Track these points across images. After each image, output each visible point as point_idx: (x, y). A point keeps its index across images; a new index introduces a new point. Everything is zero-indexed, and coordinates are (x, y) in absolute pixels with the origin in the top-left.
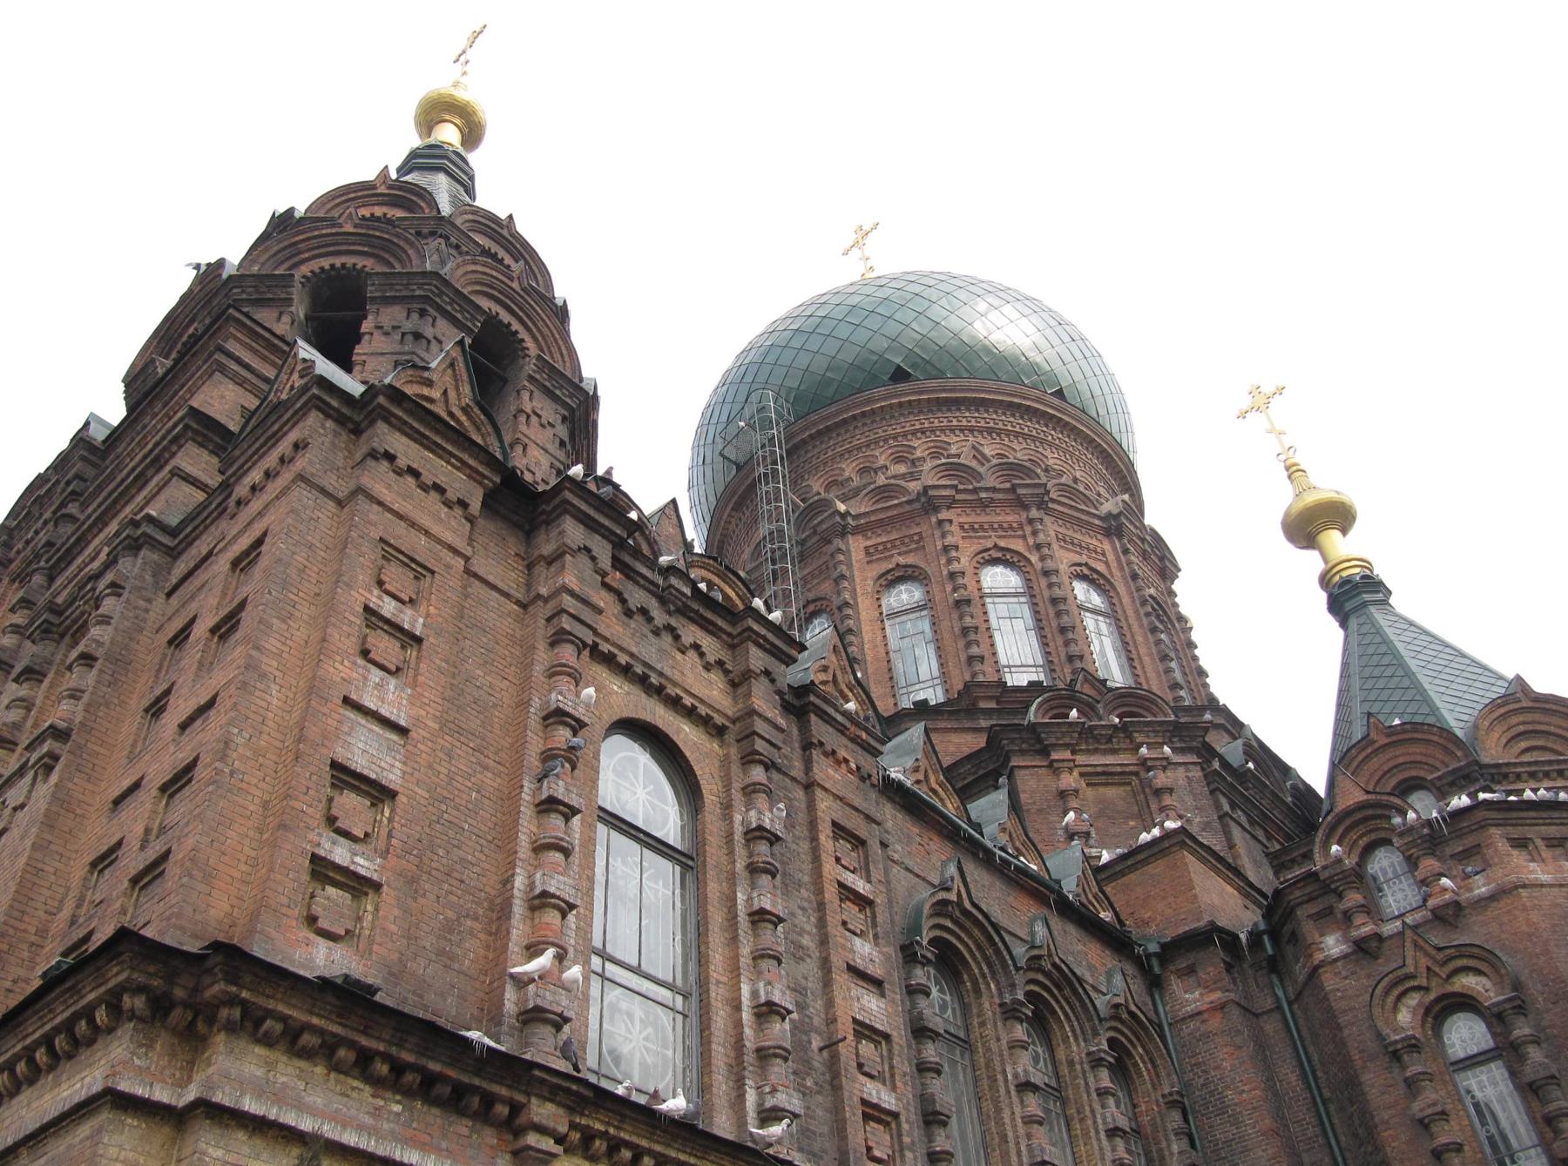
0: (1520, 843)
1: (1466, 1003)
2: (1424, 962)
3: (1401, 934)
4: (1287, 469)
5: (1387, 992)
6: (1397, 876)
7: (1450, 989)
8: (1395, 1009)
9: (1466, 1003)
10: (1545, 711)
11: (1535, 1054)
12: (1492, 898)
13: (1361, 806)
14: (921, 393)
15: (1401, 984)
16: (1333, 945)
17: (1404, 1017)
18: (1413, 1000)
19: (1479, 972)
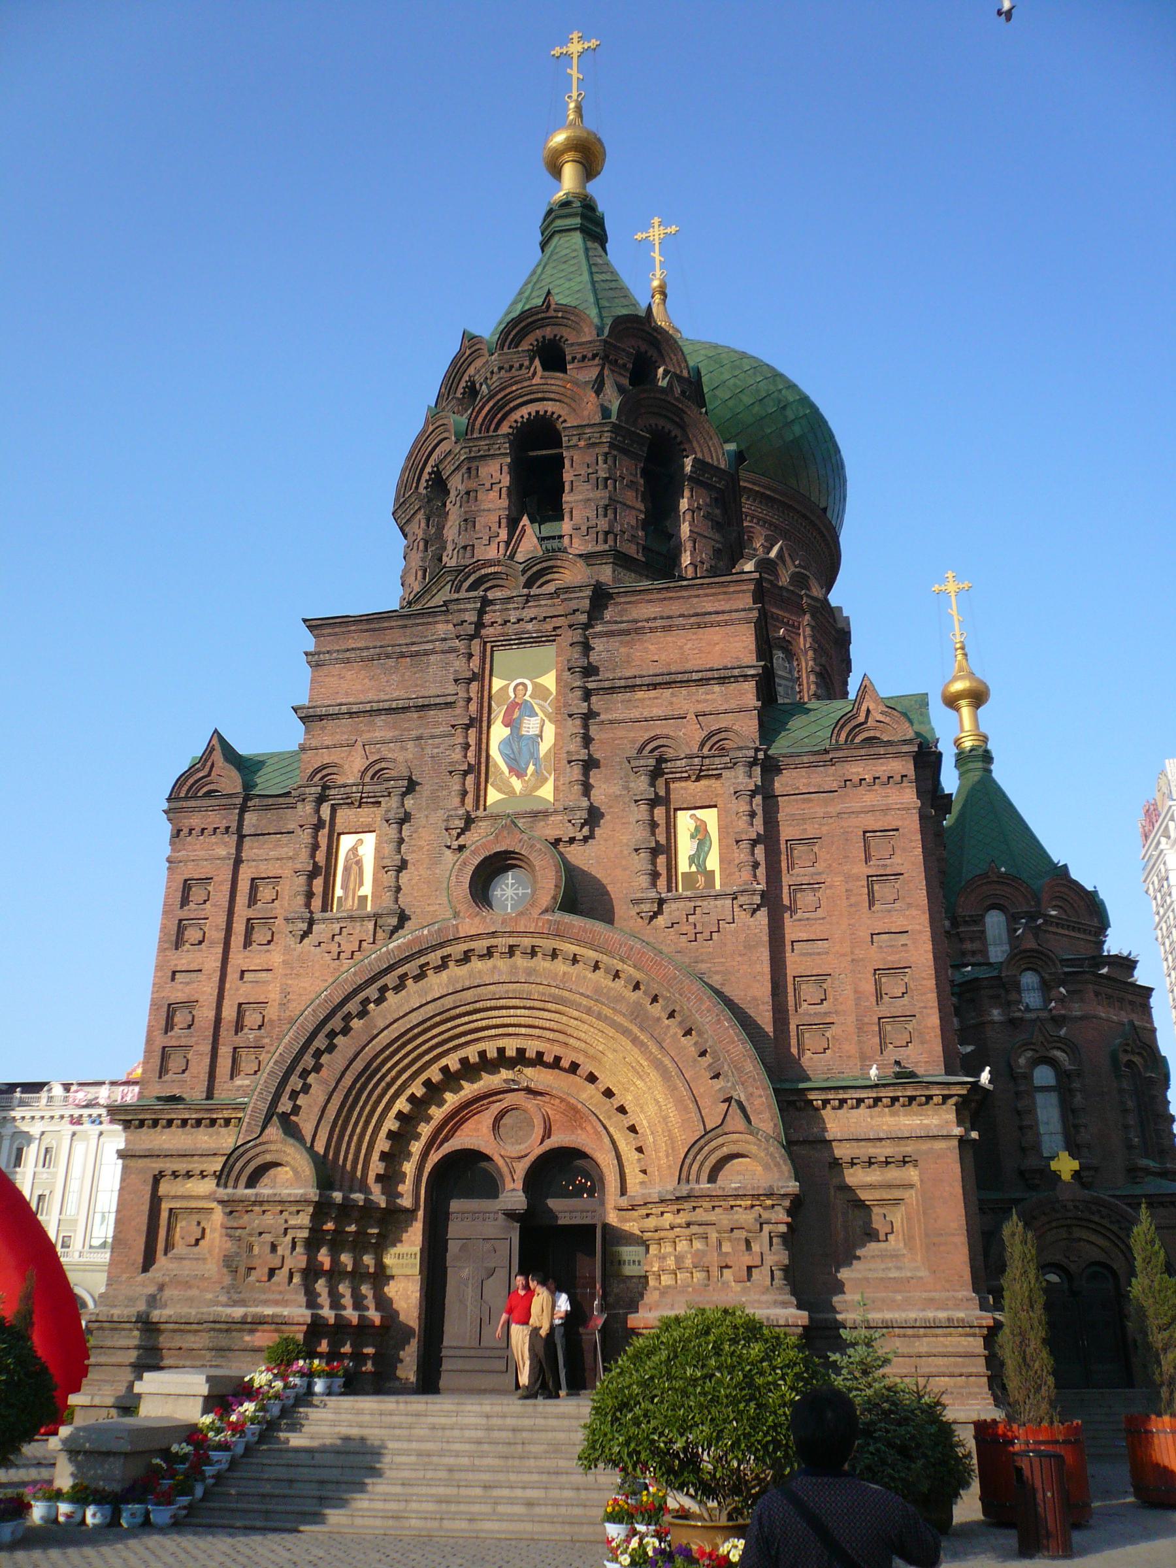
0: (1097, 994)
1: (1052, 1062)
2: (1041, 1039)
3: (1034, 1020)
5: (1020, 1047)
6: (1033, 989)
7: (1047, 1054)
8: (1020, 1057)
9: (1052, 1062)
10: (1070, 888)
11: (1078, 1099)
12: (1082, 1018)
13: (1032, 950)
14: (754, 484)
15: (1027, 1045)
16: (996, 1014)
17: (1022, 1061)
18: (1029, 1054)
19: (1064, 1051)
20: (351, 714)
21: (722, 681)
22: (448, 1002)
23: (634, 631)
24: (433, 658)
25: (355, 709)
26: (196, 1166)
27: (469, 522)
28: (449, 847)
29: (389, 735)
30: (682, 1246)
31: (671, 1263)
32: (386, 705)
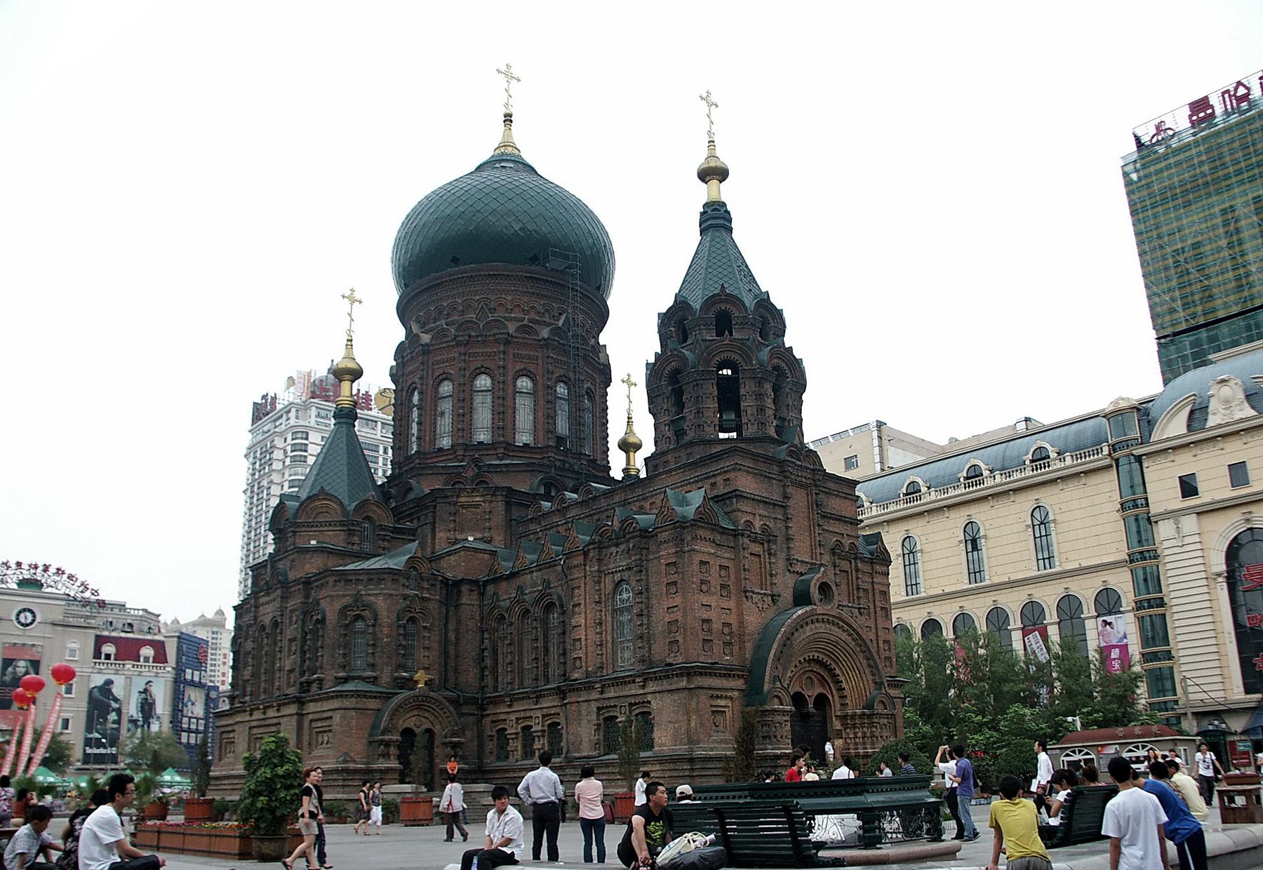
4: (629, 418)
20: (753, 499)
21: (851, 523)
22: (811, 638)
23: (828, 493)
24: (774, 481)
25: (756, 497)
26: (724, 694)
27: (761, 410)
28: (789, 570)
29: (767, 514)
30: (865, 729)
31: (859, 735)
32: (765, 500)
